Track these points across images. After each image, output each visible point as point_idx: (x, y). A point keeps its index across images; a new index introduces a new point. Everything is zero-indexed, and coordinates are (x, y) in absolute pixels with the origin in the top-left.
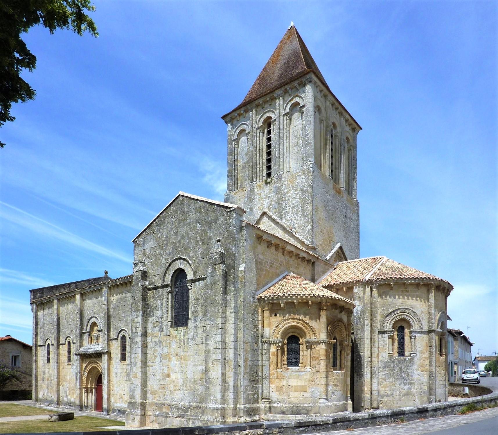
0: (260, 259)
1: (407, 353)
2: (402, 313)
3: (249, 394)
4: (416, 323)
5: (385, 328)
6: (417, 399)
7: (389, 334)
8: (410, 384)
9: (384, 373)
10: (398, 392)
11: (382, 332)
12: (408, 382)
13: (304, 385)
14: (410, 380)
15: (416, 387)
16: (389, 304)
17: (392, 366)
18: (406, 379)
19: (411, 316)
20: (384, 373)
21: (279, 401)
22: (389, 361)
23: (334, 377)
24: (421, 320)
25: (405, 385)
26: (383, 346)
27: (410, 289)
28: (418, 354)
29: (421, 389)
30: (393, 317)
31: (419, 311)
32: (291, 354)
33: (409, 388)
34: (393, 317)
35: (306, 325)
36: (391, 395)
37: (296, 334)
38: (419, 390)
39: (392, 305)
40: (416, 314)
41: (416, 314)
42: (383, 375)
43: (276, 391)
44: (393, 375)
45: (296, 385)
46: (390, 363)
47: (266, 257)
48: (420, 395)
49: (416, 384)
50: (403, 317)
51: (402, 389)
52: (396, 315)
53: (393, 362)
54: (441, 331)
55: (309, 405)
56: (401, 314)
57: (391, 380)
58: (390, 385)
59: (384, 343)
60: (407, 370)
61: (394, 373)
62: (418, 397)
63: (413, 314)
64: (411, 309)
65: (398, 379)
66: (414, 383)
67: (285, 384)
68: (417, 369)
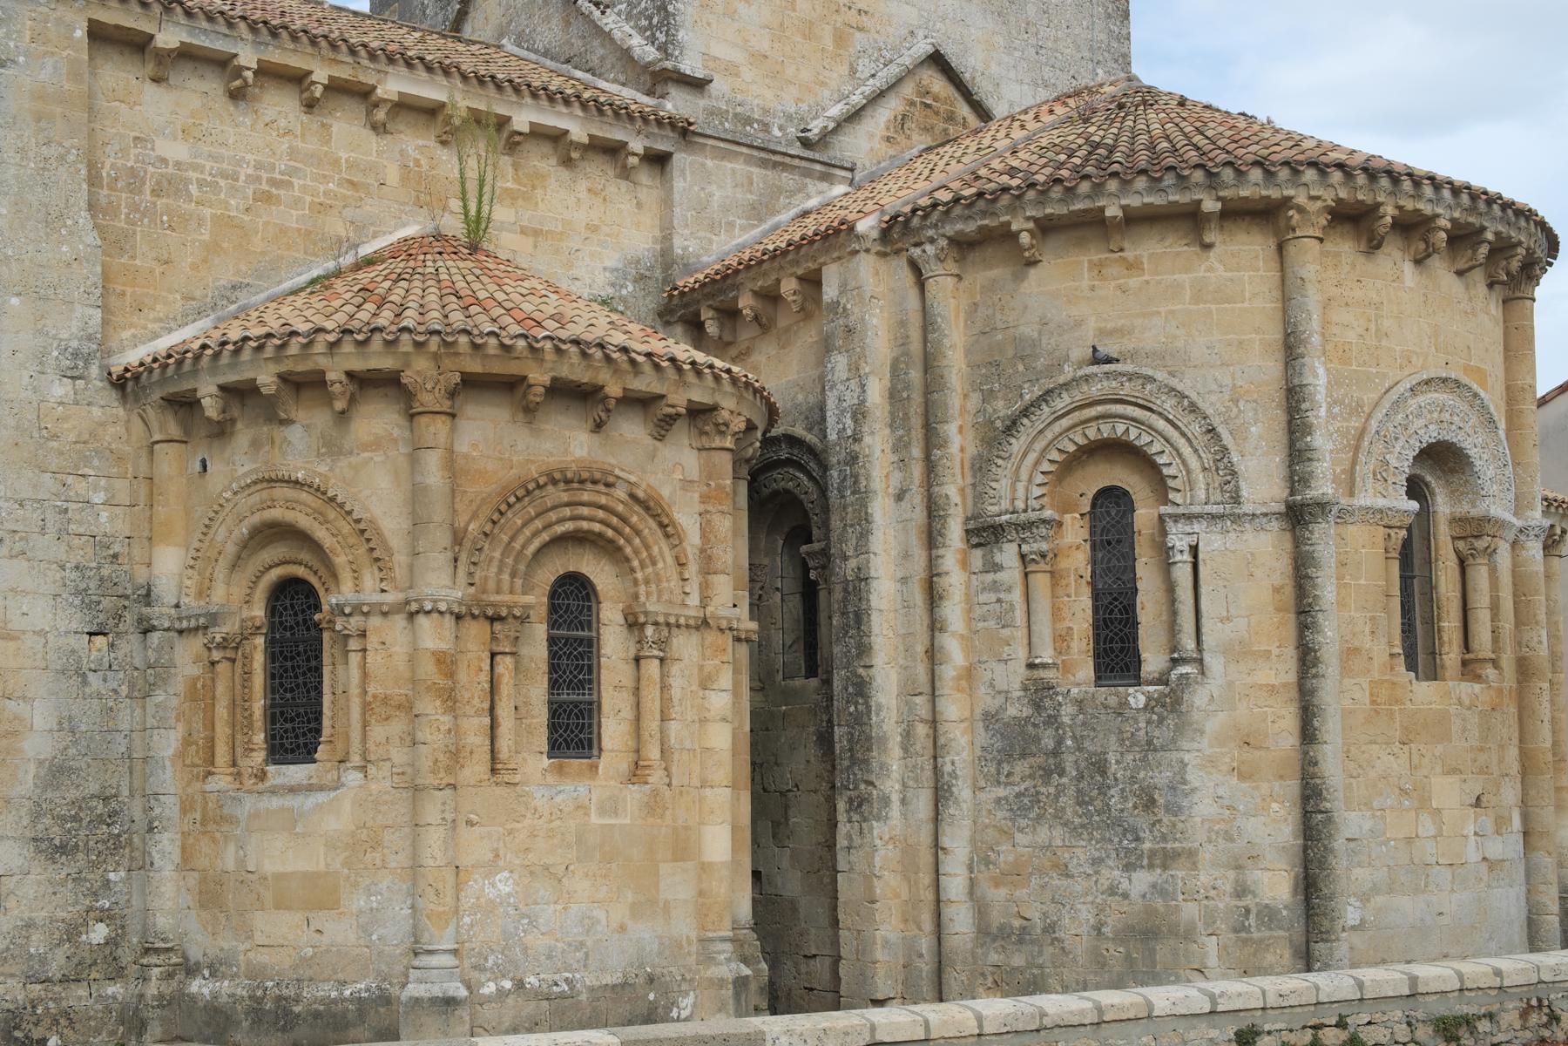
0: (164, 161)
1: (1153, 660)
3: (29, 925)
4: (1194, 463)
6: (1212, 961)
8: (1166, 859)
10: (1086, 914)
11: (985, 534)
12: (1147, 845)
13: (322, 867)
14: (1164, 838)
15: (1204, 878)
16: (1022, 358)
17: (1048, 742)
19: (1161, 424)
20: (1001, 792)
21: (210, 966)
23: (527, 822)
24: (1227, 439)
25: (1128, 868)
26: (992, 624)
27: (1149, 248)
28: (1214, 662)
29: (1241, 891)
30: (1049, 435)
31: (1214, 387)
32: (292, 690)
33: (1154, 886)
34: (1049, 435)
35: (332, 514)
36: (1045, 930)
37: (300, 571)
38: (1224, 903)
39: (1041, 363)
40: (1193, 408)
41: (1192, 404)
42: (998, 801)
43: (202, 906)
44: (1057, 797)
45: (279, 868)
46: (1035, 725)
47: (223, 151)
48: (1236, 931)
49: (1206, 855)
51: (1112, 891)
52: (1065, 422)
53: (1053, 721)
54: (1414, 505)
55: (347, 993)
57: (1043, 834)
58: (1041, 871)
59: (999, 601)
60: (1137, 769)
61: (1060, 790)
62: (1223, 949)
63: (1168, 404)
64: (1160, 375)
65: (1083, 826)
66: (1191, 854)
67: (230, 865)
68: (1211, 762)
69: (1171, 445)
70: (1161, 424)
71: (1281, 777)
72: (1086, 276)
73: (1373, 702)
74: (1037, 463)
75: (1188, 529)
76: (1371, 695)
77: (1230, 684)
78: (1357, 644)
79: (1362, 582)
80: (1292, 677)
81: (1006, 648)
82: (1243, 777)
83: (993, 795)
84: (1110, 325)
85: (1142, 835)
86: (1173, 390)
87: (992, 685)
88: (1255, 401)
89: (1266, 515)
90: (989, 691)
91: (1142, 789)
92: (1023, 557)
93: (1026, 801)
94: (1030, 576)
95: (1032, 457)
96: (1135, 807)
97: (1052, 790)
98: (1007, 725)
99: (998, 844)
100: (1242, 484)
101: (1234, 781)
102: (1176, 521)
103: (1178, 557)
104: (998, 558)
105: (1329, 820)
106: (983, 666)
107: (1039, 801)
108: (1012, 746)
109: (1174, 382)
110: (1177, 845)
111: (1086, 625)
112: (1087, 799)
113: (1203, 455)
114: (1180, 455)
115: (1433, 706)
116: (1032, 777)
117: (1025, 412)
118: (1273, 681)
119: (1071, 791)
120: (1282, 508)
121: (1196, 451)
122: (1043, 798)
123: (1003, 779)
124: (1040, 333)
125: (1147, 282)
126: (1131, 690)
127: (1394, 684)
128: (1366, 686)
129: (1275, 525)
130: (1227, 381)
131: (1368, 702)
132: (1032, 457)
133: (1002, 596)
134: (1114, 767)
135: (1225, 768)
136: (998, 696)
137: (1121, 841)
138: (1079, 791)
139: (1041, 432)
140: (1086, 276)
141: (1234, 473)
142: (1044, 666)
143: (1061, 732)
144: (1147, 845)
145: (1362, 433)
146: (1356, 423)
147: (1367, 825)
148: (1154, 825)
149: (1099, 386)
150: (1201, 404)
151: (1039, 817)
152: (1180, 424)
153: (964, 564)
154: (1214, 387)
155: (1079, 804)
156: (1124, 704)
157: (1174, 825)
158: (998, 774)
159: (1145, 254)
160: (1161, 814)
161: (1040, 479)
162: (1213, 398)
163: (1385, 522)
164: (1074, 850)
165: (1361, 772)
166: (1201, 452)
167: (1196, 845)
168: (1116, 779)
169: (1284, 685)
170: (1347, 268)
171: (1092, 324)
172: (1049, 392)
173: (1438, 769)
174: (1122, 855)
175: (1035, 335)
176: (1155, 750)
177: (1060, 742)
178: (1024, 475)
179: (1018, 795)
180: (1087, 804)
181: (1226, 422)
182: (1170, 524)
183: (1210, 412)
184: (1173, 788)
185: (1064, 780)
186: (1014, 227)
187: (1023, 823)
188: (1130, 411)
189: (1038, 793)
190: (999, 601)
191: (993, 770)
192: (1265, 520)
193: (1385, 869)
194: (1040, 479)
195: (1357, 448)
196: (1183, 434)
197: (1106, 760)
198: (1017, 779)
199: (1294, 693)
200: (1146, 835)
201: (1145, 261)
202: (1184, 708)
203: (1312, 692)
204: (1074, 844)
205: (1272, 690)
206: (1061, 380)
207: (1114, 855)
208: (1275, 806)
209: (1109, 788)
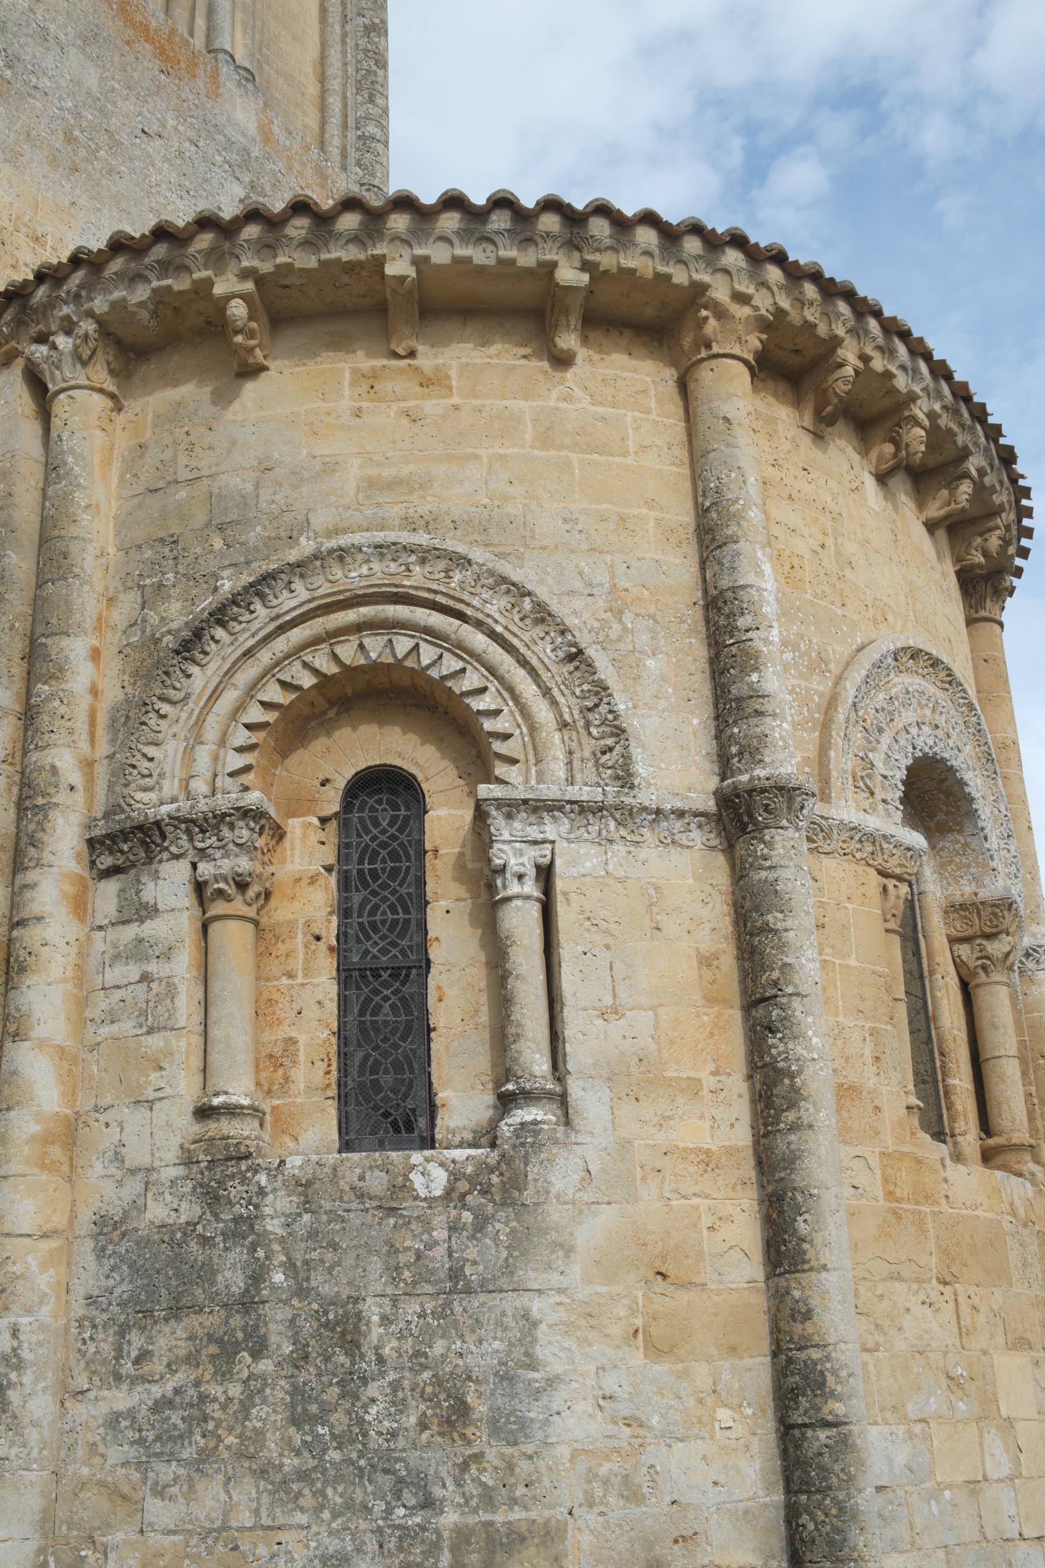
2: (364, 610)
4: (543, 712)
5: (170, 787)
7: (202, 852)
9: (121, 1399)
12: (450, 1518)
14: (488, 1499)
16: (221, 528)
18: (420, 1482)
19: (479, 641)
20: (121, 1399)
22: (190, 1211)
24: (605, 671)
26: (127, 1026)
30: (265, 657)
31: (578, 585)
34: (265, 657)
39: (254, 535)
40: (542, 615)
42: (113, 1421)
44: (245, 1409)
46: (205, 1241)
50: (375, 646)
52: (298, 635)
56: (351, 616)
59: (145, 978)
60: (427, 1335)
64: (478, 555)
65: (303, 1475)
69: (500, 679)
70: (479, 641)
71: (733, 1349)
72: (347, 392)
73: (890, 1195)
74: (240, 708)
75: (533, 833)
76: (886, 1180)
77: (624, 1145)
78: (853, 1077)
79: (852, 962)
80: (742, 1136)
81: (154, 1076)
82: (655, 1350)
83: (103, 1409)
84: (387, 473)
85: (438, 1492)
86: (504, 580)
87: (118, 1158)
88: (652, 617)
89: (680, 814)
90: (112, 1170)
91: (438, 1381)
92: (199, 887)
93: (175, 1418)
94: (215, 928)
95: (230, 697)
96: (423, 1425)
97: (235, 1390)
98: (144, 1243)
99: (107, 1526)
100: (636, 752)
101: (637, 1358)
102: (509, 816)
103: (514, 888)
104: (149, 892)
105: (844, 1444)
106: (103, 1118)
107: (205, 1419)
108: (152, 1290)
109: (505, 568)
110: (517, 1515)
111: (324, 1034)
112: (314, 1408)
113: (561, 700)
114: (516, 698)
115: (979, 1212)
116: (191, 1360)
117: (220, 616)
118: (707, 1142)
119: (279, 1392)
120: (711, 805)
121: (546, 692)
122: (213, 1410)
123: (127, 1368)
124: (257, 486)
125: (456, 408)
126: (417, 1157)
127: (919, 1162)
128: (875, 1162)
129: (697, 837)
130: (602, 577)
131: (880, 1193)
132: (230, 697)
133: (152, 967)
134: (377, 1331)
135: (617, 1330)
136: (129, 1181)
137: (389, 1511)
138: (296, 1391)
139: (248, 653)
140: (347, 392)
141: (619, 732)
142: (232, 1111)
143: (261, 1253)
144: (450, 1518)
145: (832, 702)
146: (821, 686)
147: (901, 1456)
148: (464, 1467)
149: (364, 570)
150: (554, 606)
151: (205, 1456)
152: (515, 642)
153: (80, 906)
154: (578, 585)
155: (296, 1421)
156: (401, 1188)
157: (511, 1467)
158: (119, 1357)
159: (454, 364)
160: (481, 1438)
161: (242, 737)
162: (578, 603)
163: (878, 861)
164: (281, 1536)
165: (881, 1339)
166: (556, 692)
167: (560, 1513)
168: (381, 1360)
169: (730, 1151)
170: (786, 446)
171: (353, 472)
172: (268, 577)
173: (1000, 1339)
174: (392, 1545)
175: (249, 487)
176: (468, 1291)
177: (257, 1277)
178: (211, 732)
179: (160, 1406)
180: (320, 1419)
181: (603, 645)
182: (497, 821)
183: (571, 621)
184: (507, 1378)
185: (266, 1366)
186: (218, 290)
187: (166, 1471)
188: (422, 615)
189: (203, 1398)
190: (145, 978)
191: (107, 1349)
192: (678, 825)
193: (941, 1553)
194: (242, 737)
195: (826, 725)
196: (523, 663)
197: (359, 1316)
198: (157, 1366)
199: (748, 1170)
200: (446, 1492)
201: (453, 374)
202: (529, 1196)
203: (791, 1161)
204: (281, 1520)
205: (707, 1160)
206: (293, 555)
207: (372, 1546)
208: (724, 1415)
209: (364, 1380)
